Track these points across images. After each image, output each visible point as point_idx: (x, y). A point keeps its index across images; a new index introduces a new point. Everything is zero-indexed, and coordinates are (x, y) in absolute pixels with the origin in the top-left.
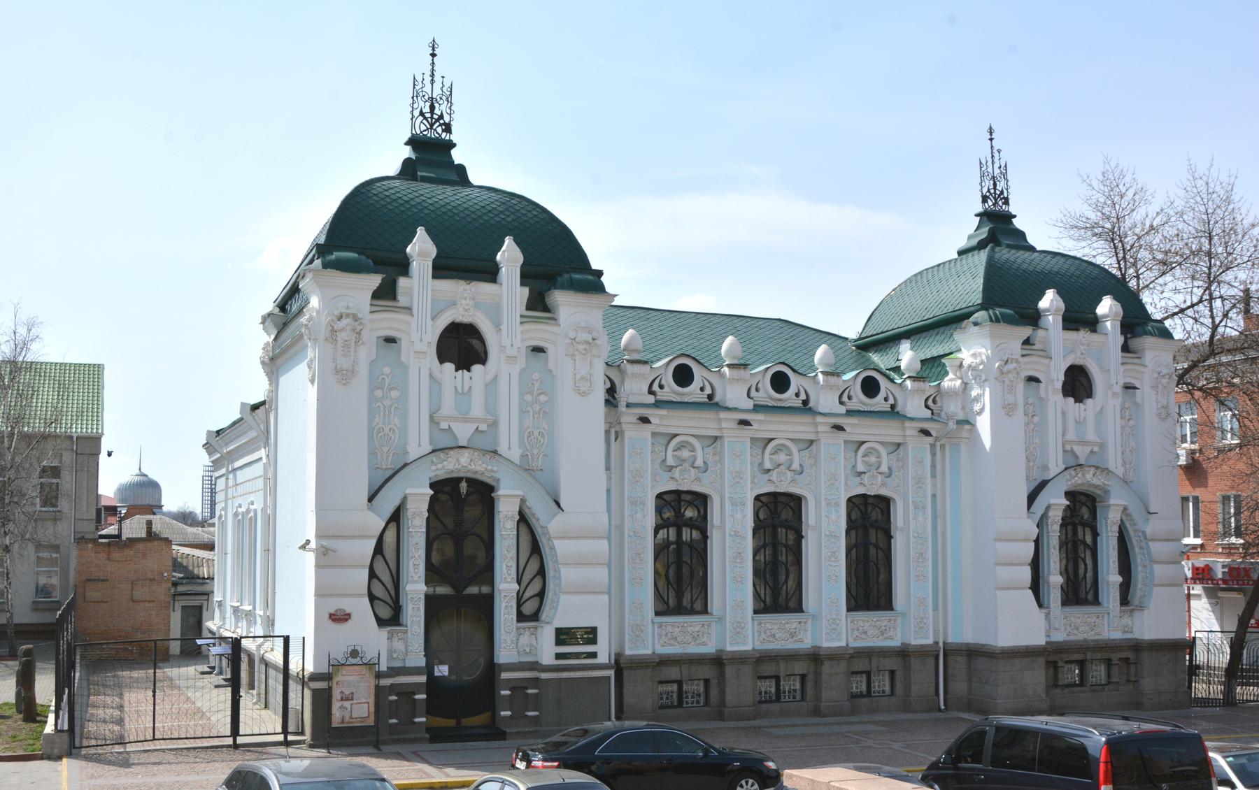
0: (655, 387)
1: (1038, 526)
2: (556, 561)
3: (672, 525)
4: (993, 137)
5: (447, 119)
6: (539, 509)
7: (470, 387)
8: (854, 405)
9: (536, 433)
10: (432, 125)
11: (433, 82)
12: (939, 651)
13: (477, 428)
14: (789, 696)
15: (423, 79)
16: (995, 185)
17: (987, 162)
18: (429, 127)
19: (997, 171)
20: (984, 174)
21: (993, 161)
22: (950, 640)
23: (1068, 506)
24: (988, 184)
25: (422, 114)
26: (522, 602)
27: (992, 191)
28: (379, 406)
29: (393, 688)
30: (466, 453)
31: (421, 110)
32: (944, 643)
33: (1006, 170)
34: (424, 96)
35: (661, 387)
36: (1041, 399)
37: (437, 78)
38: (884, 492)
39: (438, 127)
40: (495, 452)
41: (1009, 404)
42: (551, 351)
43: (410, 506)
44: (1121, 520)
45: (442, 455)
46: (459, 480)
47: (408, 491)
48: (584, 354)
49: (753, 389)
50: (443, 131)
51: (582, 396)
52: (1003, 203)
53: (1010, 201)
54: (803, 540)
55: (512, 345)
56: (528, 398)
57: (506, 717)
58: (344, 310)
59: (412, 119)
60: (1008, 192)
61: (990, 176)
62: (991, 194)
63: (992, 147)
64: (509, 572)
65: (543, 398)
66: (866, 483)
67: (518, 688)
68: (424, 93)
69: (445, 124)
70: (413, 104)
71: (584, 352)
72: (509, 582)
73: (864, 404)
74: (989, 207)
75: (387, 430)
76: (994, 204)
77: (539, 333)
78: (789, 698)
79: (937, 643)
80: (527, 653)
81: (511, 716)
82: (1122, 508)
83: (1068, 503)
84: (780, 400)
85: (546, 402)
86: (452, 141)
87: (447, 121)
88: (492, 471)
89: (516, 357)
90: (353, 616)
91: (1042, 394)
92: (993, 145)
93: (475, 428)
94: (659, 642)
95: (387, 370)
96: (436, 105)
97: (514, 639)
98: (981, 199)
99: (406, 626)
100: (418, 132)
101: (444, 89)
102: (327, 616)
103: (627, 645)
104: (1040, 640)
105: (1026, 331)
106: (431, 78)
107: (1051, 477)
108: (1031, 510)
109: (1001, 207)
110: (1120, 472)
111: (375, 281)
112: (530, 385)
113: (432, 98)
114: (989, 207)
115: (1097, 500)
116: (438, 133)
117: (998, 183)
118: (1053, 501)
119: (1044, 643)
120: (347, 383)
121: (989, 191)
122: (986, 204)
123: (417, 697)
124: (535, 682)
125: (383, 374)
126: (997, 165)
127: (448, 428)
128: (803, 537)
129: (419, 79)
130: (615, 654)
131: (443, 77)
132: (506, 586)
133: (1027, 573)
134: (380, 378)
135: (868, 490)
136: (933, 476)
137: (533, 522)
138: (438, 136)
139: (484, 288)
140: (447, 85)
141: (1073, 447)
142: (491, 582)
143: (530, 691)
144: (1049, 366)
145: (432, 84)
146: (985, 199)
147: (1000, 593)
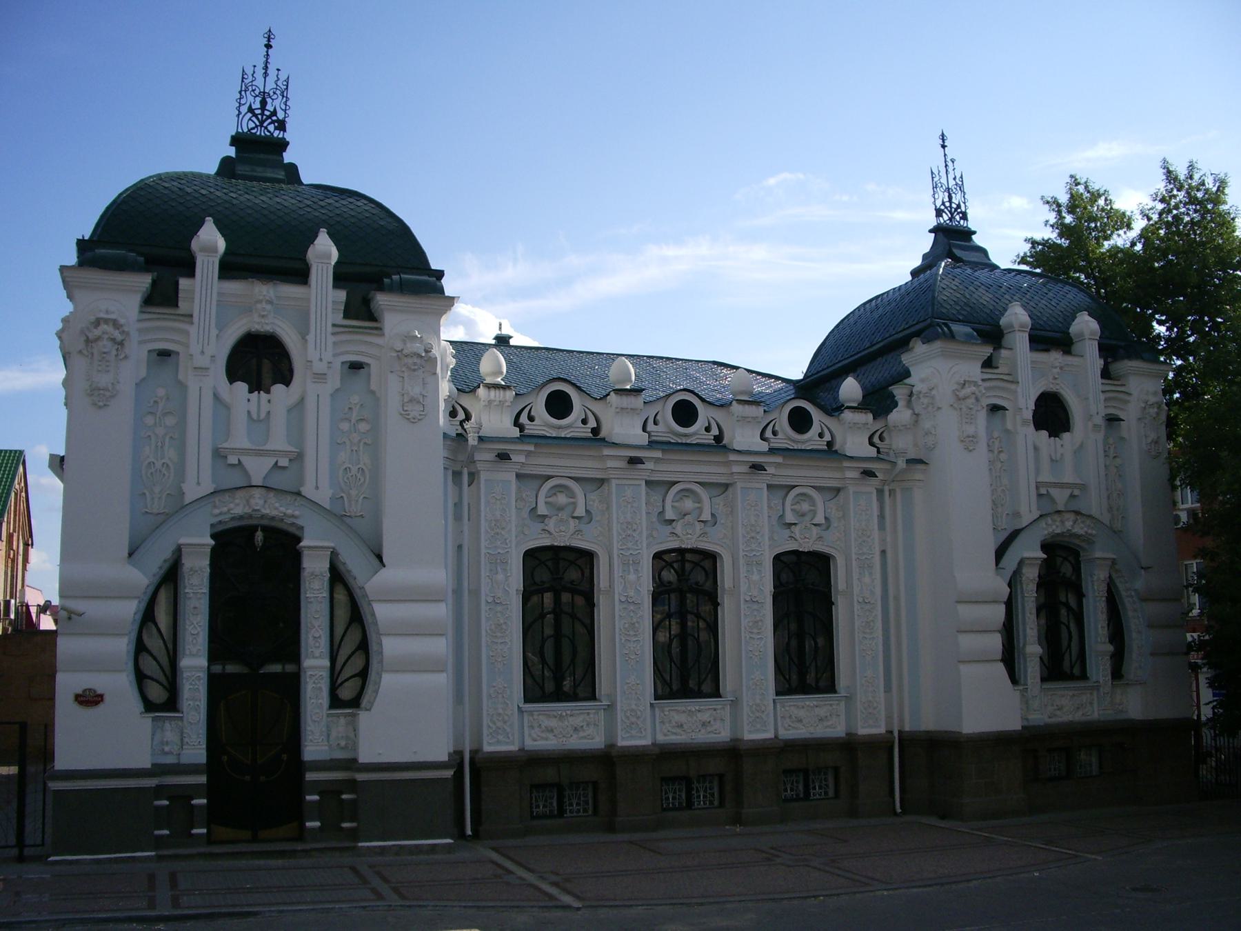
0: (524, 419)
1: (1010, 585)
2: (379, 634)
3: (548, 590)
4: (946, 144)
5: (281, 115)
6: (355, 563)
7: (269, 413)
8: (779, 443)
9: (354, 470)
10: (262, 122)
11: (266, 75)
12: (893, 742)
13: (277, 462)
14: (704, 802)
15: (254, 72)
16: (950, 198)
17: (939, 172)
18: (258, 124)
19: (952, 183)
20: (936, 185)
21: (947, 171)
22: (907, 728)
23: (1045, 559)
24: (942, 196)
25: (251, 110)
26: (339, 681)
27: (947, 204)
28: (149, 436)
29: (159, 791)
30: (257, 493)
31: (250, 106)
32: (900, 732)
33: (962, 181)
34: (253, 91)
35: (531, 419)
36: (1007, 431)
39: (269, 124)
40: (299, 494)
41: (969, 437)
42: (374, 369)
43: (188, 563)
44: (1110, 577)
45: (227, 497)
46: (253, 529)
47: (182, 541)
48: (414, 370)
49: (651, 421)
50: (276, 128)
51: (413, 422)
52: (961, 218)
53: (969, 216)
54: (719, 607)
55: (321, 360)
56: (345, 426)
57: (313, 829)
58: (102, 315)
59: (238, 115)
60: (966, 206)
61: (944, 188)
62: (946, 208)
63: (945, 155)
64: (317, 644)
65: (363, 427)
66: (798, 537)
67: (330, 791)
68: (254, 88)
69: (278, 121)
70: (240, 99)
71: (413, 367)
72: (316, 658)
73: (794, 441)
74: (945, 221)
75: (158, 464)
76: (950, 219)
77: (359, 346)
78: (705, 804)
79: (891, 732)
80: (342, 748)
81: (320, 828)
82: (1109, 563)
83: (1045, 556)
84: (686, 435)
85: (368, 431)
86: (285, 139)
87: (281, 118)
88: (293, 516)
89: (325, 374)
90: (107, 698)
91: (1009, 426)
92: (946, 153)
93: (273, 463)
94: (530, 735)
95: (161, 392)
96: (269, 100)
97: (323, 729)
98: (935, 212)
99: (182, 713)
100: (246, 130)
101: (279, 83)
102: (72, 698)
103: (485, 740)
104: (1012, 723)
105: (987, 350)
106: (264, 71)
107: (1024, 526)
108: (1000, 566)
109: (959, 222)
110: (1106, 519)
111: (144, 281)
112: (346, 409)
113: (264, 93)
114: (945, 221)
115: (1081, 554)
116: (269, 131)
117: (953, 195)
118: (1026, 555)
119: (1020, 728)
120: (105, 405)
121: (943, 203)
122: (941, 218)
123: (195, 802)
124: (352, 785)
125: (156, 397)
126: (951, 176)
127: (237, 462)
128: (718, 604)
129: (249, 71)
130: (470, 751)
131: (278, 70)
133: (995, 642)
134: (152, 402)
135: (800, 545)
136: (882, 527)
137: (351, 582)
138: (268, 134)
139: (291, 291)
140: (283, 77)
141: (1049, 489)
142: (296, 658)
143: (344, 797)
144: (1016, 392)
145: (265, 78)
146: (939, 213)
147: (964, 668)
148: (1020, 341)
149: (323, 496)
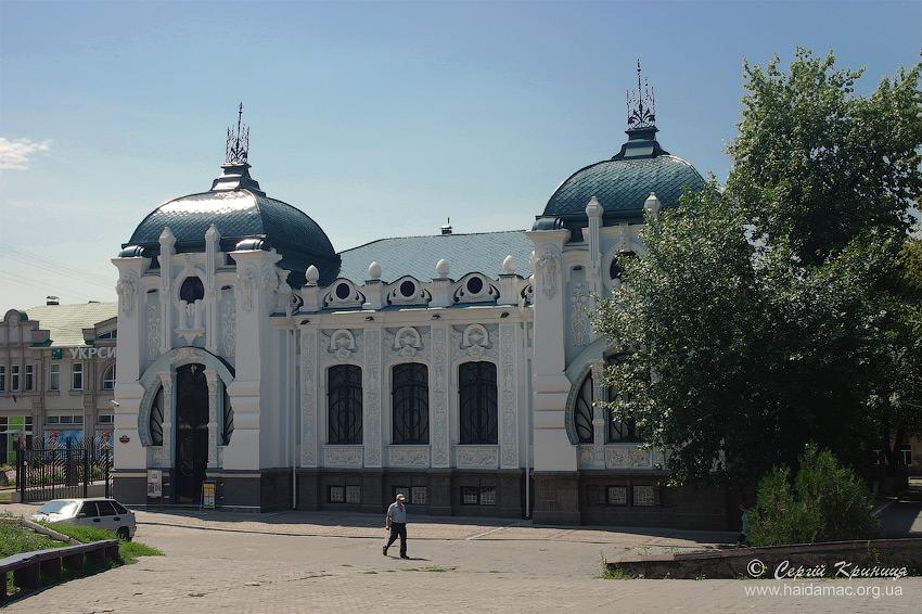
5: (245, 149)
16: (641, 107)
37: (241, 129)
38: (486, 359)
121: (635, 113)
132: (213, 426)
146: (631, 121)
148: (595, 222)
149: (214, 349)
